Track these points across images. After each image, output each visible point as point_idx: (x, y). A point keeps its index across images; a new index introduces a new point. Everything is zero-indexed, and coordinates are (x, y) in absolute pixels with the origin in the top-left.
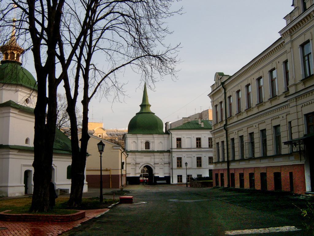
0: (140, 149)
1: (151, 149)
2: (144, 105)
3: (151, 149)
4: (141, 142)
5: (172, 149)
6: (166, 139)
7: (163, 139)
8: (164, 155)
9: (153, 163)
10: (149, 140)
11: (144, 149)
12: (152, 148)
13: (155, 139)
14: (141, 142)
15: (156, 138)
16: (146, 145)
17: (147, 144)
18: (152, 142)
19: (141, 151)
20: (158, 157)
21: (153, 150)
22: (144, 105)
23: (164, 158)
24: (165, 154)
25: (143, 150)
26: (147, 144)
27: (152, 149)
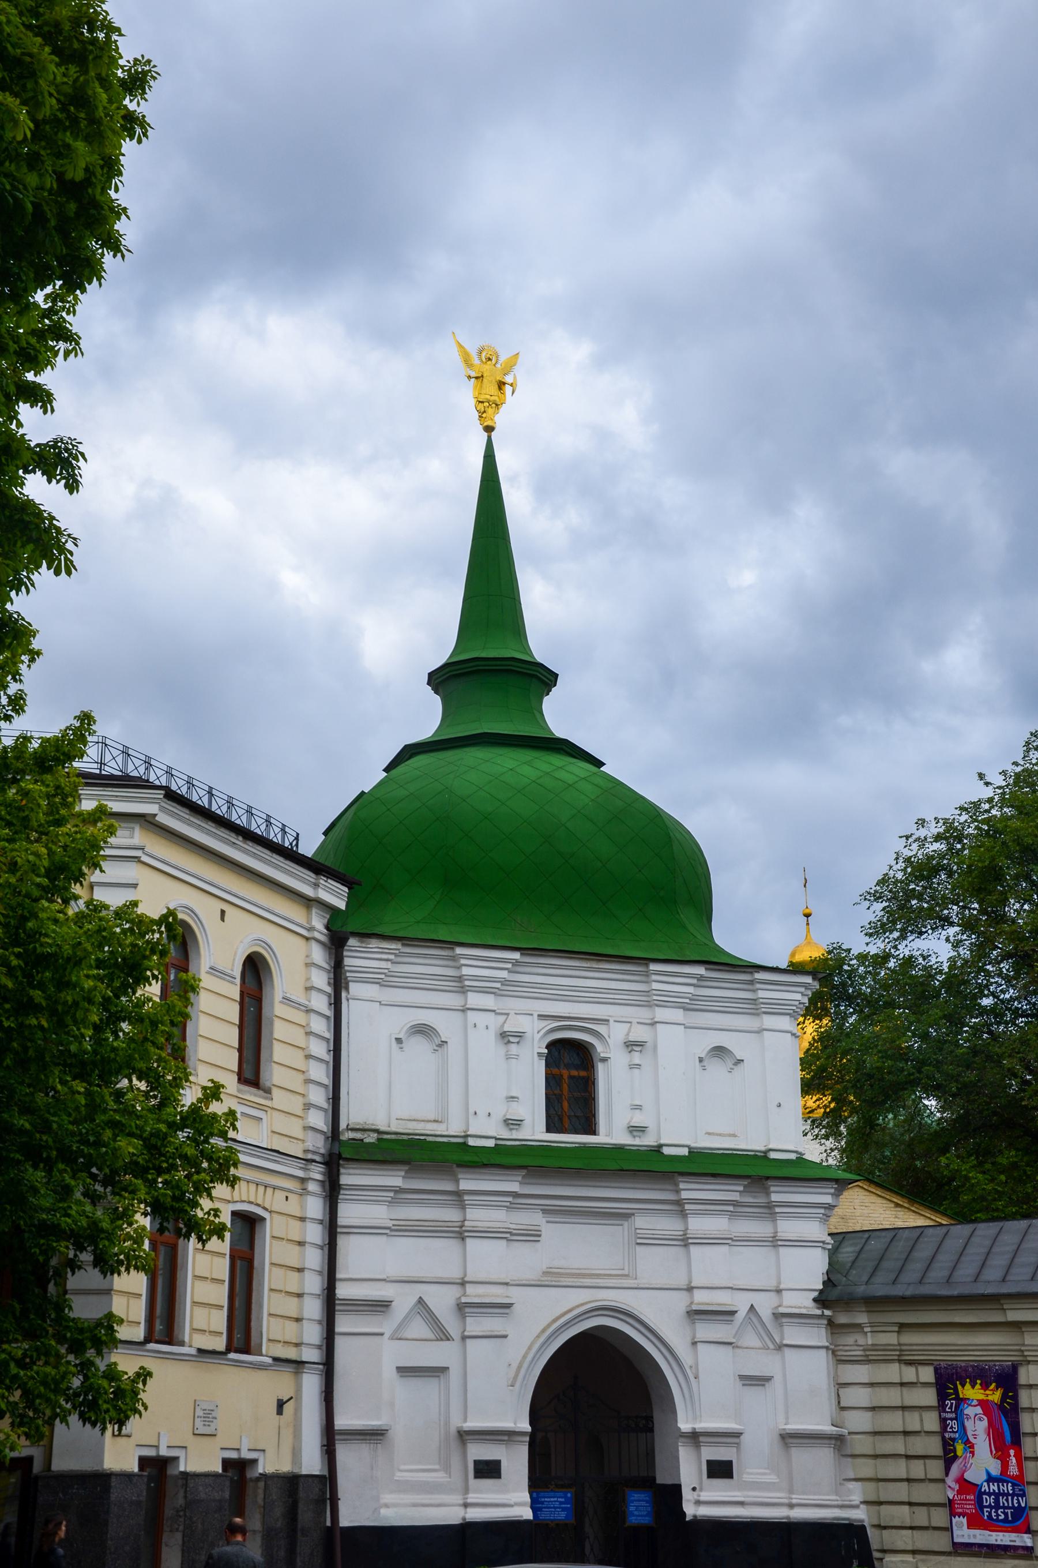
0: (485, 1130)
1: (612, 1129)
2: (492, 671)
3: (612, 1129)
4: (505, 1037)
9: (679, 1302)
11: (535, 1129)
12: (622, 1112)
14: (505, 1037)
18: (631, 1046)
19: (499, 1149)
21: (648, 1140)
22: (492, 671)
27: (636, 1130)
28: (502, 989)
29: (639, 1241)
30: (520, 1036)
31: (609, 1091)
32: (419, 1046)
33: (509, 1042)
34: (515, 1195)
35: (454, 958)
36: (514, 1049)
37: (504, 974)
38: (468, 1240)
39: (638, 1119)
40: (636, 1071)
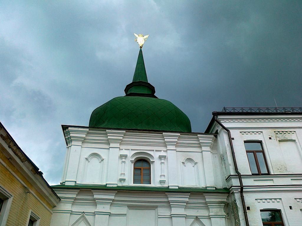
5: (239, 176)
6: (208, 149)
7: (198, 150)
8: (206, 206)
10: (151, 153)
11: (130, 182)
13: (169, 147)
15: (171, 143)
16: (135, 169)
17: (142, 164)
18: (160, 157)
20: (181, 211)
21: (166, 185)
23: (209, 218)
24: (209, 199)
25: (125, 184)
26: (142, 164)
28: (121, 142)
29: (159, 217)
30: (126, 156)
31: (154, 171)
32: (95, 161)
33: (122, 158)
34: (113, 200)
35: (106, 134)
36: (124, 160)
37: (121, 138)
38: (96, 215)
39: (163, 179)
40: (163, 165)
